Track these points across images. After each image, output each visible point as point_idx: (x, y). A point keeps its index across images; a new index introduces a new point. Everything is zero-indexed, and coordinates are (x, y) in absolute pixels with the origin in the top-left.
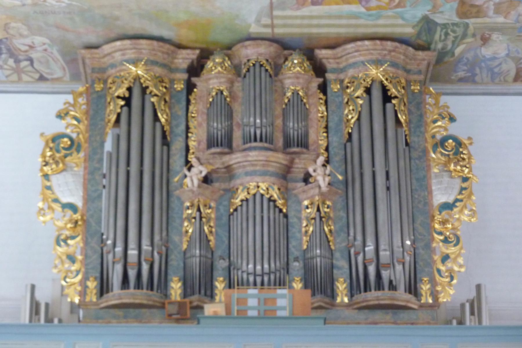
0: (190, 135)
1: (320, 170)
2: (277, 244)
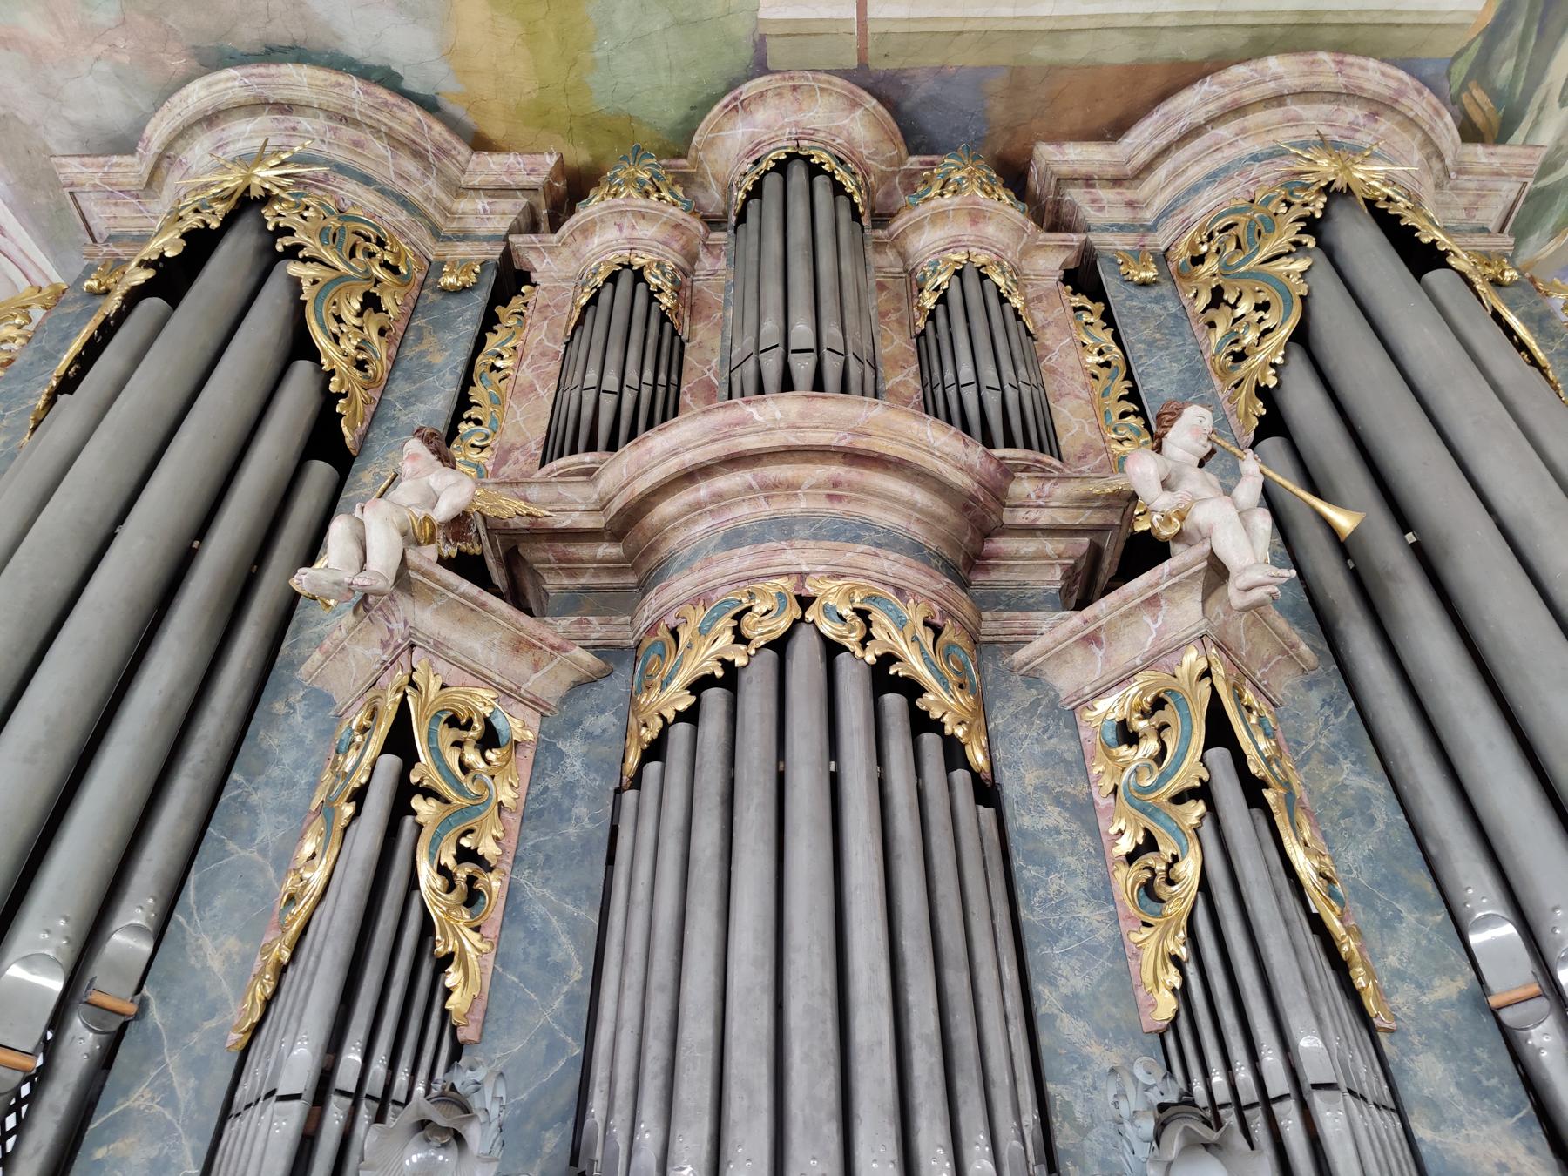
2: (957, 981)
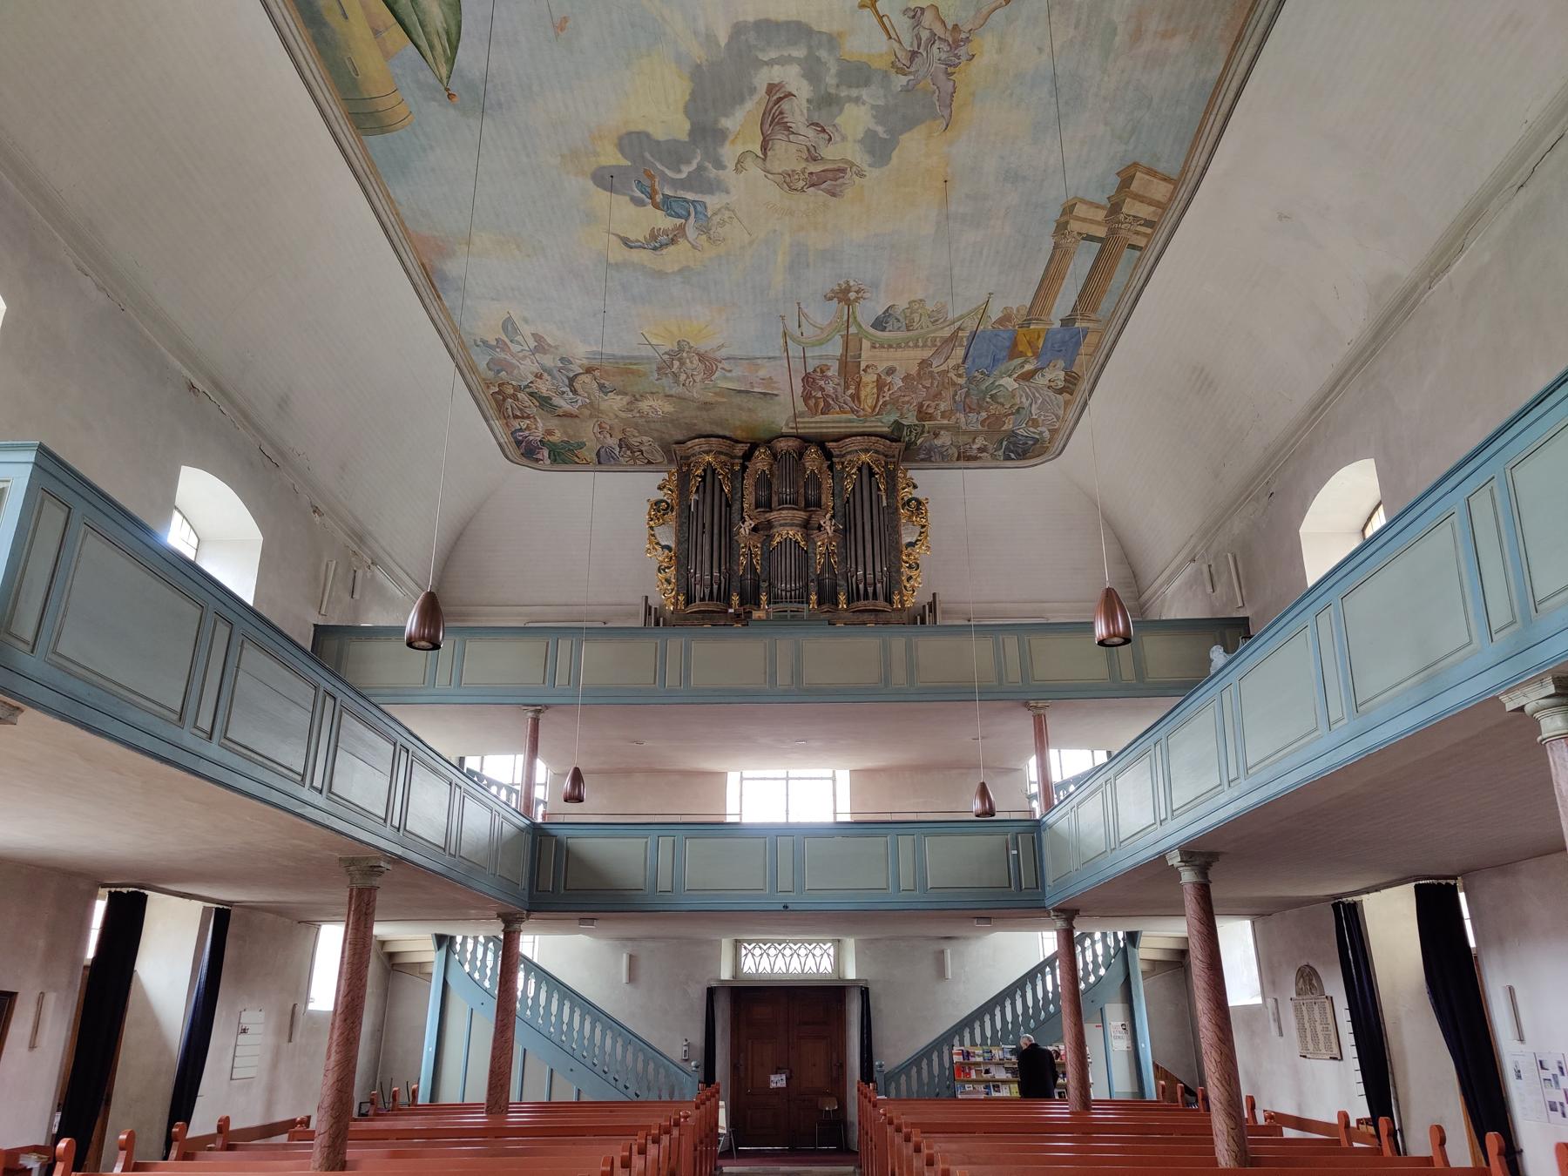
1: (828, 523)
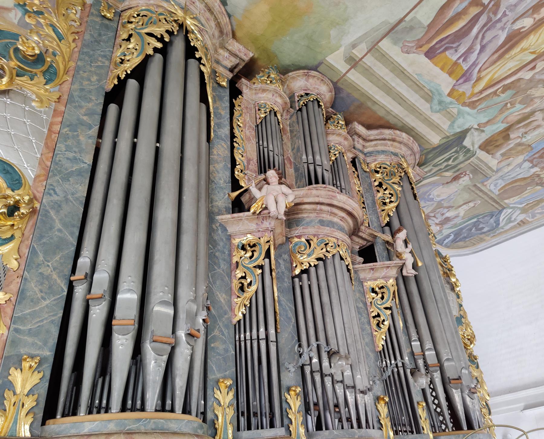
0: (235, 144)
